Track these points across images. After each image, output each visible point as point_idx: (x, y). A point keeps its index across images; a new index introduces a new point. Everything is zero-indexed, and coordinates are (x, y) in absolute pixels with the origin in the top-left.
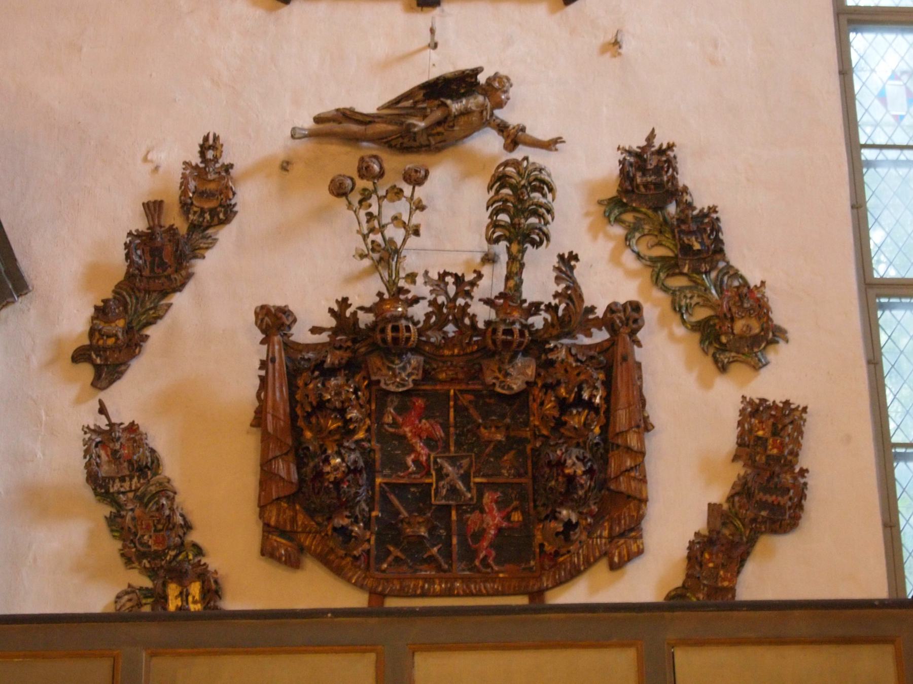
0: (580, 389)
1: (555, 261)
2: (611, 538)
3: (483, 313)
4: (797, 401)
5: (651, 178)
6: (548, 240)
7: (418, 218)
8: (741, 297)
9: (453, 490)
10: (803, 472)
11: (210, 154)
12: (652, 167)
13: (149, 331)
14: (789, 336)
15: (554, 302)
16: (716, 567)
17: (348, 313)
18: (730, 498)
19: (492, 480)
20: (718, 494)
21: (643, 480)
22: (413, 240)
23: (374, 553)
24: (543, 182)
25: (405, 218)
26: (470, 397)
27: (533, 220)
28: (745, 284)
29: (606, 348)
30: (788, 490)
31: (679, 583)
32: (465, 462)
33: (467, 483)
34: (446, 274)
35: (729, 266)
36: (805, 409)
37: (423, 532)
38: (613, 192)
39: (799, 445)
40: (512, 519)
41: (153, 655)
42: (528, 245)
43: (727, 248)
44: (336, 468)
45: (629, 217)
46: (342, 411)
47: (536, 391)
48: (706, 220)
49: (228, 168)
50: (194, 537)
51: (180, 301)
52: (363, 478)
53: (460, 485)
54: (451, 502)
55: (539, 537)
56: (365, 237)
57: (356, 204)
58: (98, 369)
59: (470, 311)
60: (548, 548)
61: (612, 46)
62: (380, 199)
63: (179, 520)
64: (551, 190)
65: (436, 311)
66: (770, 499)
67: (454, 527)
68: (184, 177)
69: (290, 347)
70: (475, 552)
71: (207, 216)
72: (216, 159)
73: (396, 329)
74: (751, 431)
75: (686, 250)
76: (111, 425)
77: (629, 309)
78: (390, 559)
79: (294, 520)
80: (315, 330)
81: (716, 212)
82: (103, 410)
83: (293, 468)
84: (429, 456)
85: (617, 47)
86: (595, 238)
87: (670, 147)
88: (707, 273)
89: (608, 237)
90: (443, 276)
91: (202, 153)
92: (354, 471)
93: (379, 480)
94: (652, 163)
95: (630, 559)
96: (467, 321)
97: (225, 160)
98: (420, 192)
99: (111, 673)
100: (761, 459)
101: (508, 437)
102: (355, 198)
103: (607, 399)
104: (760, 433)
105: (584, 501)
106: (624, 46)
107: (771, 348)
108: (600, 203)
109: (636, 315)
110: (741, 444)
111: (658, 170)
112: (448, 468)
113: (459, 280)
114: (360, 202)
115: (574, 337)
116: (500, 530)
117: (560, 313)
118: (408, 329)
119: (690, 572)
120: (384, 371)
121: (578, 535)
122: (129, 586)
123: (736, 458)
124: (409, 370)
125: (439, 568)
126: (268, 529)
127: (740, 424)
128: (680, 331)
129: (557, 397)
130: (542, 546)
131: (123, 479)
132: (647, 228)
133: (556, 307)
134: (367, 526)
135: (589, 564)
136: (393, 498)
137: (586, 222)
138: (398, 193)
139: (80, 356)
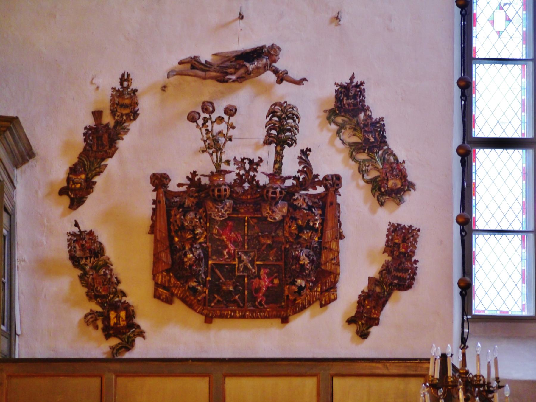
0: (309, 221)
1: (299, 154)
2: (322, 292)
3: (263, 180)
4: (415, 226)
5: (352, 101)
6: (296, 143)
7: (231, 132)
8: (392, 169)
9: (246, 268)
10: (416, 262)
11: (125, 84)
12: (352, 94)
13: (96, 179)
14: (416, 187)
15: (297, 175)
16: (371, 308)
17: (196, 179)
18: (381, 272)
19: (265, 263)
20: (374, 271)
21: (338, 264)
22: (229, 143)
23: (208, 298)
24: (293, 114)
25: (225, 132)
26: (256, 221)
27: (288, 134)
28: (396, 159)
29: (321, 197)
30: (408, 270)
31: (353, 314)
32: (252, 254)
33: (253, 265)
34: (245, 159)
35: (389, 149)
36: (419, 230)
37: (231, 289)
38: (332, 106)
39: (415, 248)
40: (274, 282)
41: (117, 376)
42: (286, 146)
43: (387, 140)
44: (190, 259)
45: (339, 120)
46: (193, 230)
47: (287, 219)
48: (378, 125)
49: (135, 91)
50: (121, 287)
51: (111, 162)
52: (203, 264)
53: (249, 266)
54: (245, 274)
55: (286, 293)
56: (205, 142)
57: (201, 126)
58: (72, 200)
59: (256, 178)
60: (291, 298)
61: (335, 19)
62: (213, 123)
63: (114, 280)
64: (298, 118)
65: (239, 178)
66: (399, 274)
67: (246, 286)
68: (112, 95)
69: (169, 195)
70: (256, 299)
71: (125, 118)
72: (128, 87)
73: (219, 191)
74: (392, 239)
75: (367, 140)
76: (80, 231)
77: (335, 178)
78: (215, 301)
79: (169, 281)
80: (180, 185)
81: (383, 121)
82: (77, 225)
83: (169, 257)
84: (234, 251)
85: (338, 20)
86: (322, 130)
87: (362, 83)
88: (377, 153)
89: (329, 130)
90: (243, 160)
91: (122, 84)
92: (198, 260)
93: (210, 262)
94: (352, 93)
95: (330, 302)
96: (254, 183)
97: (133, 86)
98: (232, 120)
99: (100, 383)
100: (396, 253)
101: (273, 242)
102: (200, 122)
103: (322, 224)
104: (397, 241)
105: (309, 275)
106: (342, 20)
107: (406, 193)
108: (325, 111)
109: (337, 182)
110: (387, 245)
111: (355, 97)
112: (244, 257)
113: (251, 162)
114: (203, 125)
115: (308, 190)
116: (268, 288)
117: (301, 180)
118: (225, 190)
119: (358, 310)
120: (214, 209)
121: (306, 292)
122: (91, 310)
123: (384, 252)
124: (226, 208)
125: (239, 306)
126: (157, 285)
127: (387, 236)
128: (362, 183)
129: (297, 224)
130: (288, 296)
131: (86, 258)
132: (348, 126)
133: (299, 178)
134: (205, 286)
135: (310, 304)
136: (217, 271)
137: (317, 122)
138: (220, 119)
139: (62, 192)
